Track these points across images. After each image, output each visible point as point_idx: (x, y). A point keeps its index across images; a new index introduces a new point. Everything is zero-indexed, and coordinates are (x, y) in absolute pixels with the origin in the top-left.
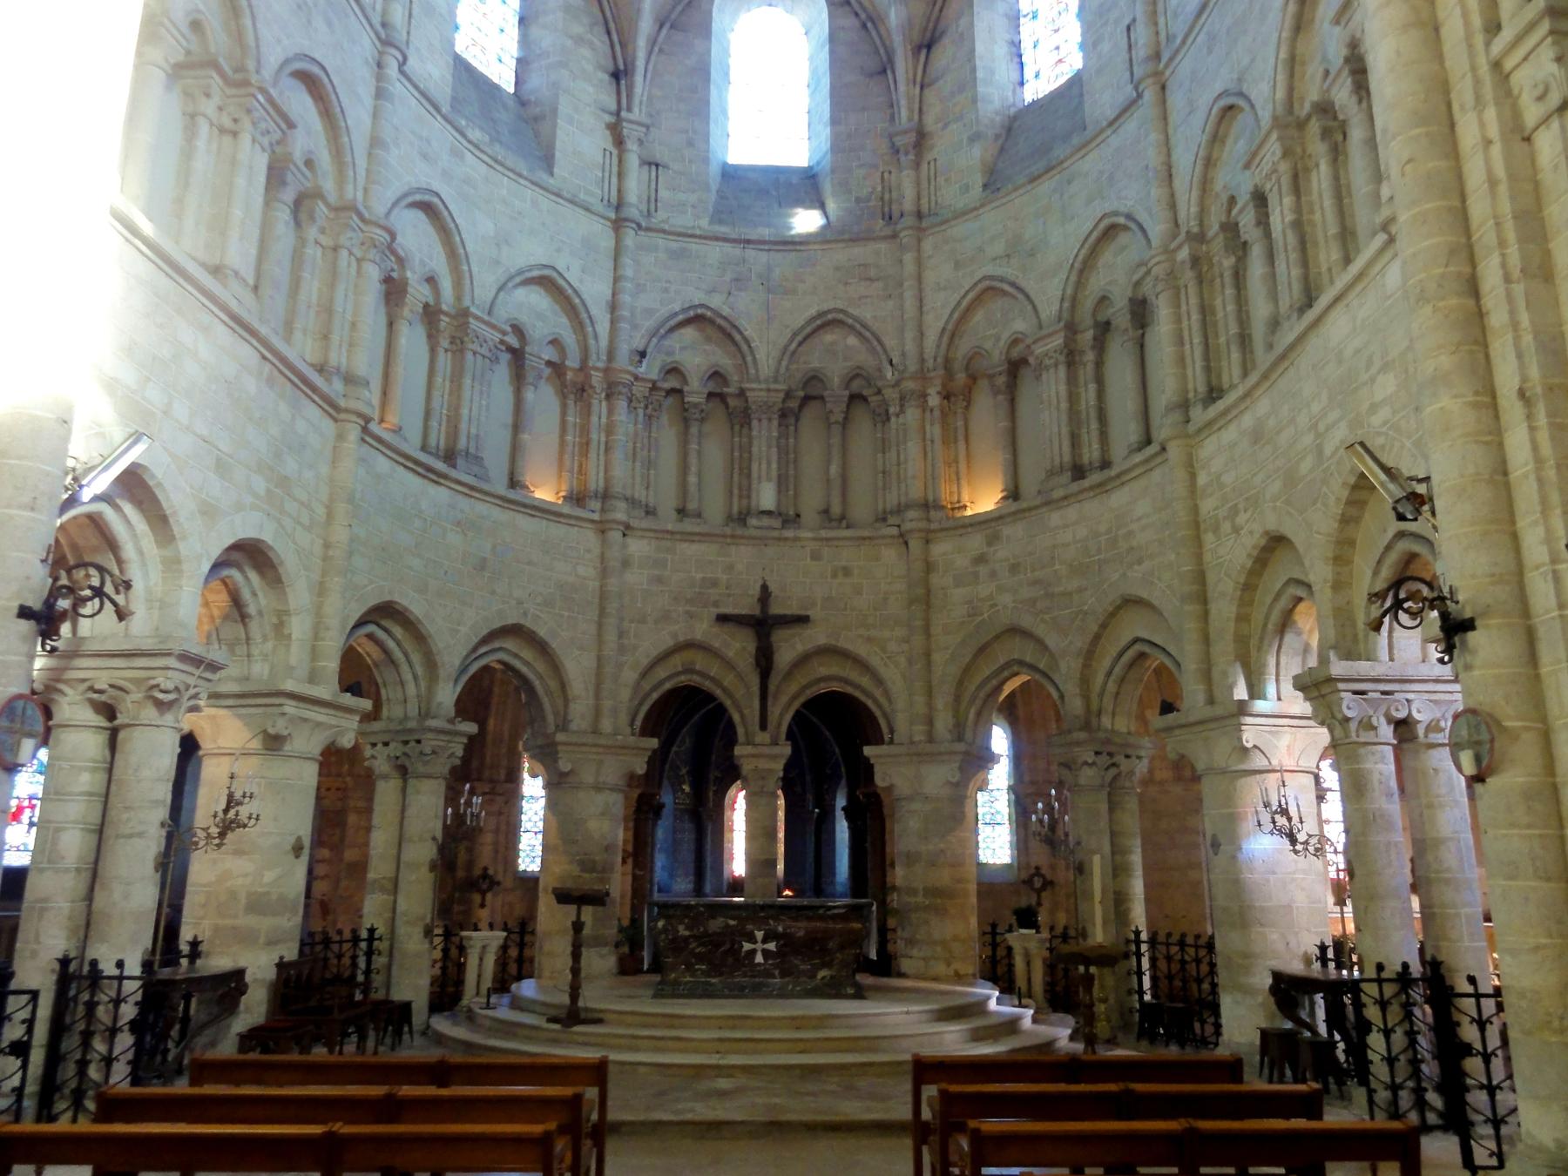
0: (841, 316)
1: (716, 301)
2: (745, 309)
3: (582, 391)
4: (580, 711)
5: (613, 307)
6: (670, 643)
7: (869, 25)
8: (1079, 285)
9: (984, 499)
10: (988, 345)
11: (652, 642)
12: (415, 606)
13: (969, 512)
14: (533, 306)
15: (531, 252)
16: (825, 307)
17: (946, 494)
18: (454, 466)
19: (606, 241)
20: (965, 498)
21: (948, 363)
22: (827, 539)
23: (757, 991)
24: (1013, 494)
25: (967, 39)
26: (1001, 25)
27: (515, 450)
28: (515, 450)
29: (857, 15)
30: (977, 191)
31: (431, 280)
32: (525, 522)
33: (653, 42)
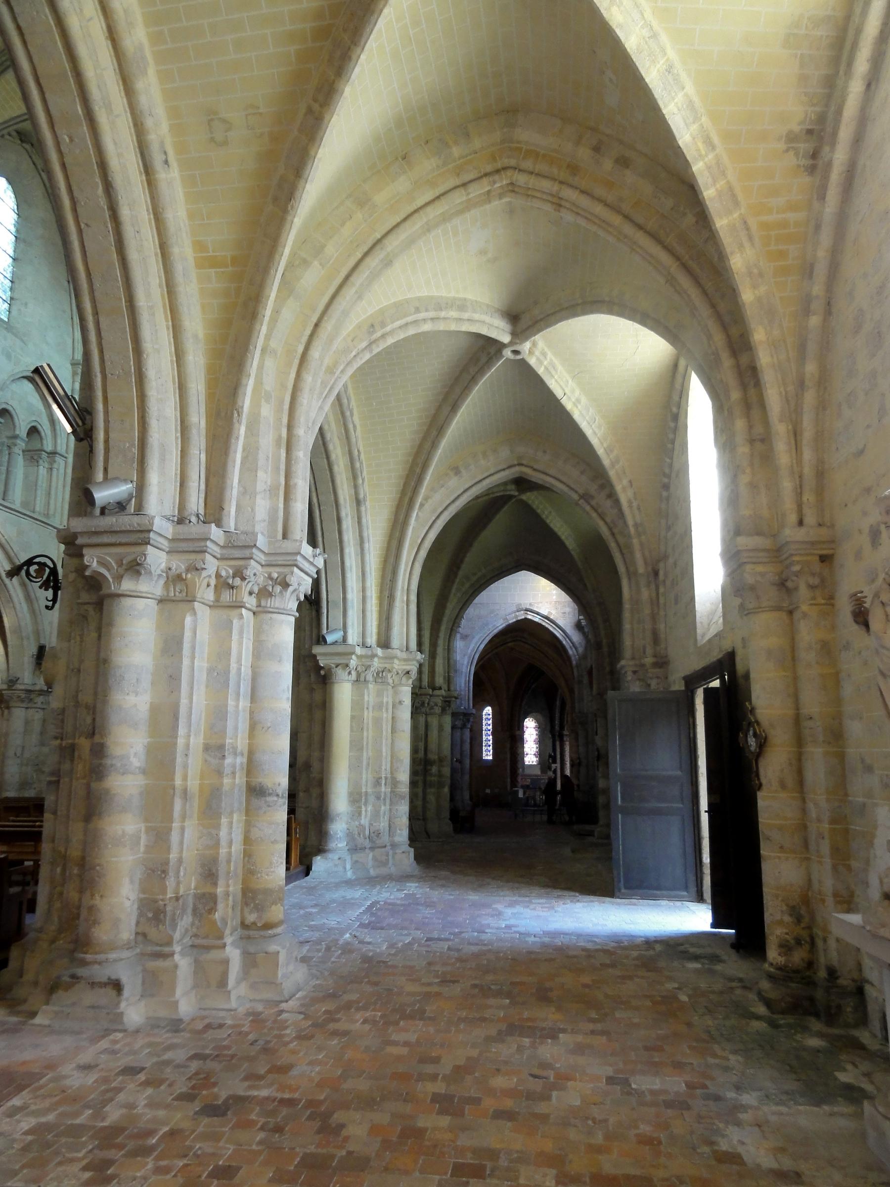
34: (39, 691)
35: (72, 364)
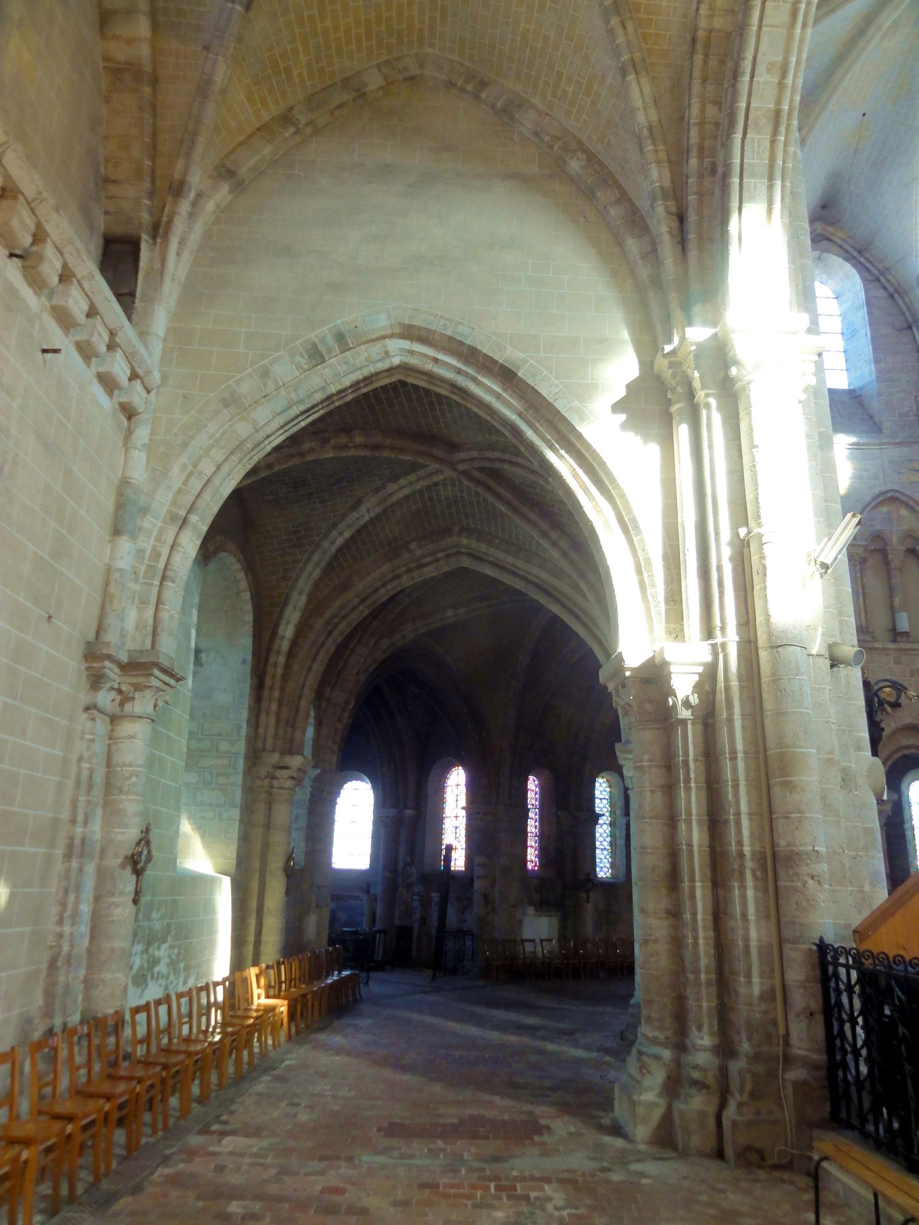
0: (898, 495)
7: (896, 296)
22: (906, 650)
29: (885, 288)
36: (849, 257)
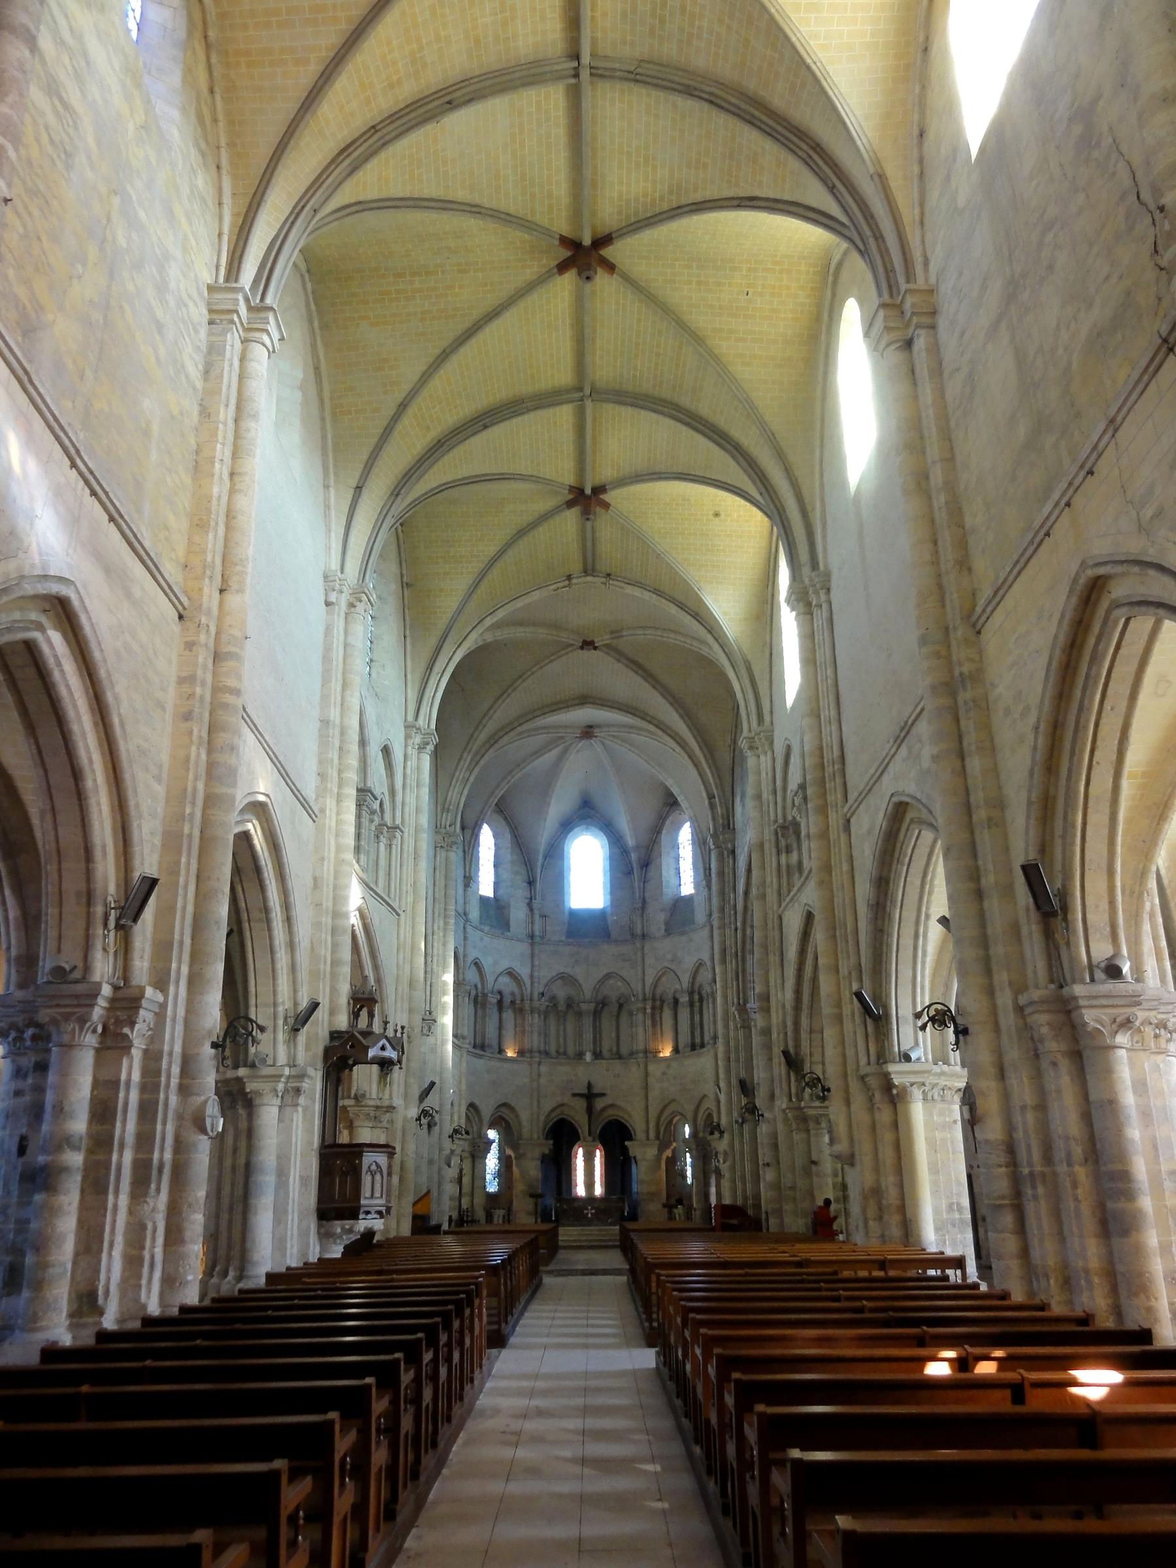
1: (569, 970)
2: (579, 972)
3: (521, 1010)
4: (526, 1132)
5: (532, 976)
6: (555, 1105)
8: (694, 978)
9: (666, 1052)
10: (667, 990)
11: (548, 1105)
12: (477, 1103)
13: (661, 1055)
14: (506, 984)
15: (504, 964)
16: (611, 970)
17: (651, 1046)
18: (484, 1051)
19: (528, 951)
20: (660, 1048)
21: (654, 995)
23: (589, 1225)
24: (676, 1050)
25: (659, 868)
26: (672, 861)
27: (500, 1036)
28: (500, 1036)
30: (663, 931)
31: (476, 986)
32: (506, 1065)
33: (543, 866)
34: (388, 1107)
35: (406, 727)
36: (601, 829)
